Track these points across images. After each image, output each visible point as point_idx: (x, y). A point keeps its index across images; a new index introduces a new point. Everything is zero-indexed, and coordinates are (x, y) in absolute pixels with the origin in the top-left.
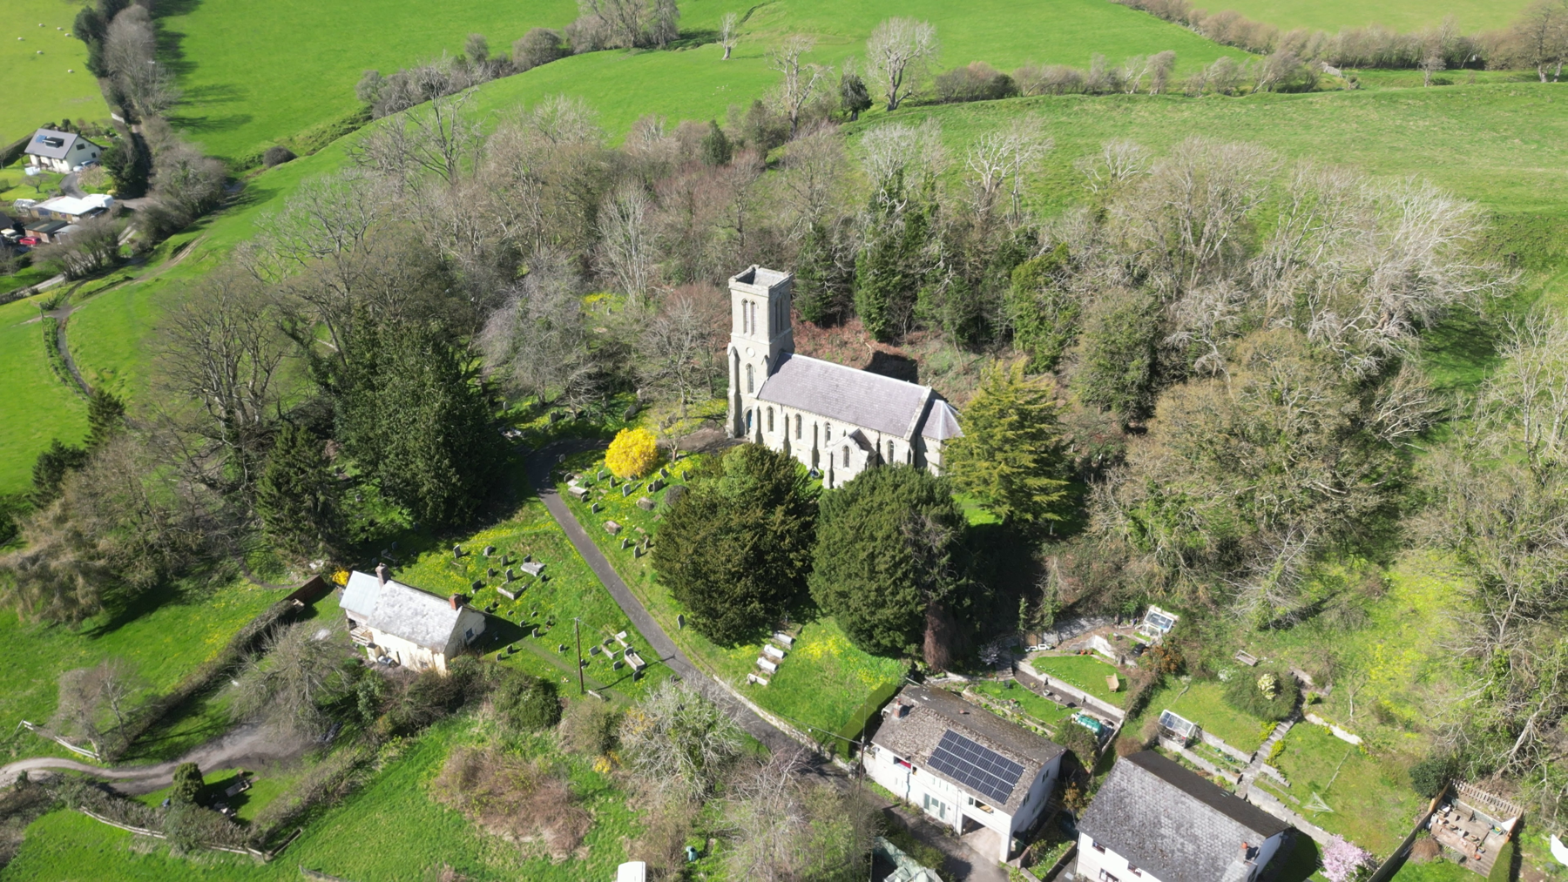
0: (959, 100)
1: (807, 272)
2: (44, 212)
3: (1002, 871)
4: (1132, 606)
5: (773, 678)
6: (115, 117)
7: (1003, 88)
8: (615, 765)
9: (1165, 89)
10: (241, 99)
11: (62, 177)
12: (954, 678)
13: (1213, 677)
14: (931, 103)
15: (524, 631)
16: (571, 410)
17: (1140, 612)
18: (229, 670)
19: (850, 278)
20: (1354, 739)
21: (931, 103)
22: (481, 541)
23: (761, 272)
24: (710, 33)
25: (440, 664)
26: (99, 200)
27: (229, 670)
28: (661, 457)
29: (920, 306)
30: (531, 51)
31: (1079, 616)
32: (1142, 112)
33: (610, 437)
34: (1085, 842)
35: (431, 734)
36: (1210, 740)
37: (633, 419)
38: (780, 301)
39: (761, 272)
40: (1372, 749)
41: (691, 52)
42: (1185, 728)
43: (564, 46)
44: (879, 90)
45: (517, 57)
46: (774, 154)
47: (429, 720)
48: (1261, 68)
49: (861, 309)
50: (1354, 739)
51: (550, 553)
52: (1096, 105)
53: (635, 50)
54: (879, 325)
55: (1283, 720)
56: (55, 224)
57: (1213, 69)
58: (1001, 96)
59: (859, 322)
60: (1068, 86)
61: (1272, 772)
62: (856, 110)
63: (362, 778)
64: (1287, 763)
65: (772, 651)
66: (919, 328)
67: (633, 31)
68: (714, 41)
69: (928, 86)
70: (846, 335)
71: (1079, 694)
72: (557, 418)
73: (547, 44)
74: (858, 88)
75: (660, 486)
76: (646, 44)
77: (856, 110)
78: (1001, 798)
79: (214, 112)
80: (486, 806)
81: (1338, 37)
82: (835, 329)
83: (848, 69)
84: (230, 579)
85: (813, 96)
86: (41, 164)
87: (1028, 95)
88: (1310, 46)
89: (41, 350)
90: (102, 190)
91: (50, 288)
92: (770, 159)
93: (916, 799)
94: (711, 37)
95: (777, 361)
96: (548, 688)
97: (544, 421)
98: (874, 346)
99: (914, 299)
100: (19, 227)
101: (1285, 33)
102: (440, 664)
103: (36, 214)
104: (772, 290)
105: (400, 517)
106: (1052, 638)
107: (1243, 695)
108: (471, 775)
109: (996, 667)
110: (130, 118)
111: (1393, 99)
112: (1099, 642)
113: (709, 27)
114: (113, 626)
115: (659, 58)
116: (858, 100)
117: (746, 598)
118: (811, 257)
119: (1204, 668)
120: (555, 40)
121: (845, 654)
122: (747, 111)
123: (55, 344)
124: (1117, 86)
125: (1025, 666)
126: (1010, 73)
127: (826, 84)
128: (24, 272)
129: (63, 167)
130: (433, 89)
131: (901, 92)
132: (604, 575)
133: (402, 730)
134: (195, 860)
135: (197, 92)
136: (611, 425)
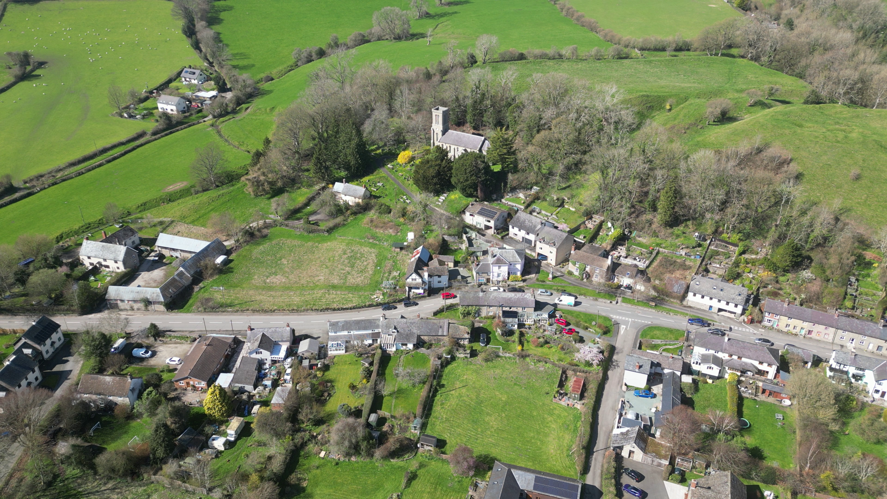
0: (506, 61)
1: (453, 110)
2: (197, 96)
3: (492, 235)
4: (529, 186)
5: (442, 203)
6: (205, 64)
7: (522, 57)
8: (405, 220)
9: (576, 58)
10: (249, 58)
11: (195, 85)
12: (486, 203)
13: (546, 200)
14: (498, 62)
15: (380, 197)
16: (387, 149)
17: (531, 188)
18: (307, 204)
19: (465, 111)
20: (574, 210)
21: (498, 62)
22: (366, 179)
23: (440, 108)
24: (422, 34)
25: (360, 201)
26: (214, 93)
27: (307, 204)
28: (412, 159)
29: (485, 119)
30: (355, 41)
31: (516, 189)
32: (565, 65)
33: (398, 154)
34: (510, 227)
35: (360, 216)
36: (543, 212)
37: (404, 150)
38: (445, 115)
39: (440, 108)
40: (577, 211)
41: (415, 42)
42: (537, 210)
43: (366, 38)
44: (480, 57)
45: (350, 44)
46: (445, 78)
47: (360, 213)
48: (610, 50)
49: (468, 121)
50: (574, 210)
51: (385, 181)
52: (551, 63)
53: (394, 41)
54: (473, 125)
55: (559, 207)
56: (202, 101)
57: (593, 51)
58: (521, 60)
59: (468, 125)
60: (544, 57)
61: (554, 216)
62: (472, 64)
63: (345, 223)
64: (559, 215)
65: (442, 198)
66: (485, 126)
67: (393, 34)
68: (423, 37)
69: (496, 56)
70: (465, 128)
71: (514, 204)
72: (383, 150)
73: (360, 38)
74: (473, 57)
75: (413, 165)
76: (398, 38)
77: (472, 64)
78: (492, 218)
79: (241, 63)
80: (376, 227)
81: (641, 40)
82: (461, 127)
83: (470, 51)
84: (300, 188)
85: (458, 59)
86: (186, 80)
87: (531, 59)
88: (632, 42)
89: (217, 137)
90: (213, 90)
91: (209, 119)
92: (444, 79)
93: (475, 224)
94: (423, 36)
95: (444, 132)
96: (389, 207)
97: (380, 151)
98: (472, 131)
99: (483, 117)
100: (190, 102)
101: (625, 38)
102: (360, 201)
103: (194, 97)
104: (443, 112)
105: (343, 173)
106: (510, 195)
107: (552, 204)
108: (372, 221)
109: (496, 200)
110: (211, 64)
111: (651, 62)
112: (521, 195)
113: (422, 32)
114: (273, 197)
115: (403, 44)
116: (473, 61)
117: (435, 184)
118: (454, 105)
119: (544, 198)
120: (364, 36)
121: (460, 198)
122: (436, 64)
123: (220, 135)
124: (561, 56)
125: (503, 200)
126: (524, 52)
127: (462, 55)
128: (200, 114)
129: (196, 82)
130: (321, 54)
131: (487, 58)
132: (399, 184)
133: (355, 214)
134: (311, 235)
135: (234, 55)
136: (398, 152)
